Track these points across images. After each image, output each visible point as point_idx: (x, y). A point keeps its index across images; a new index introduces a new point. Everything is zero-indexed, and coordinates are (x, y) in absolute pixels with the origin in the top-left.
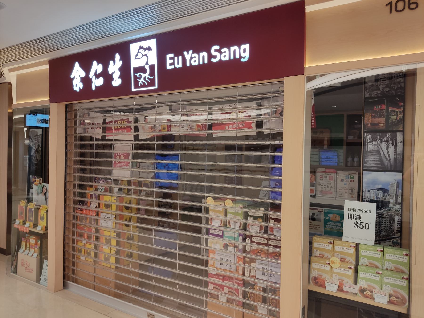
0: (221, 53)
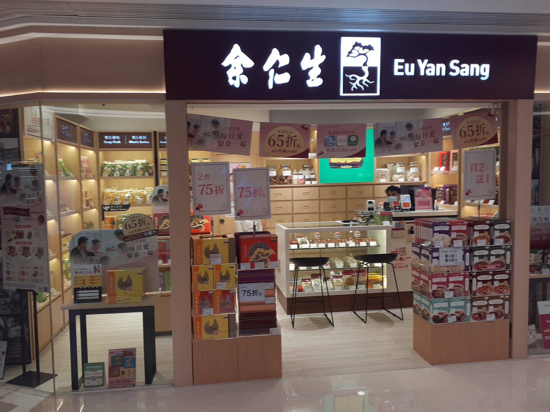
0: (461, 68)
